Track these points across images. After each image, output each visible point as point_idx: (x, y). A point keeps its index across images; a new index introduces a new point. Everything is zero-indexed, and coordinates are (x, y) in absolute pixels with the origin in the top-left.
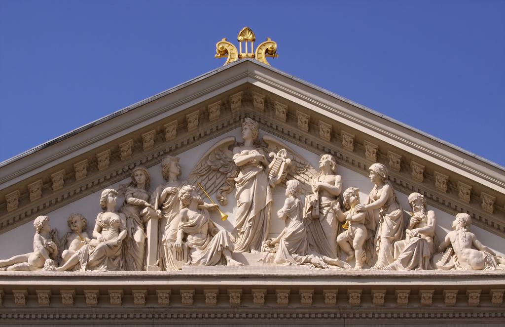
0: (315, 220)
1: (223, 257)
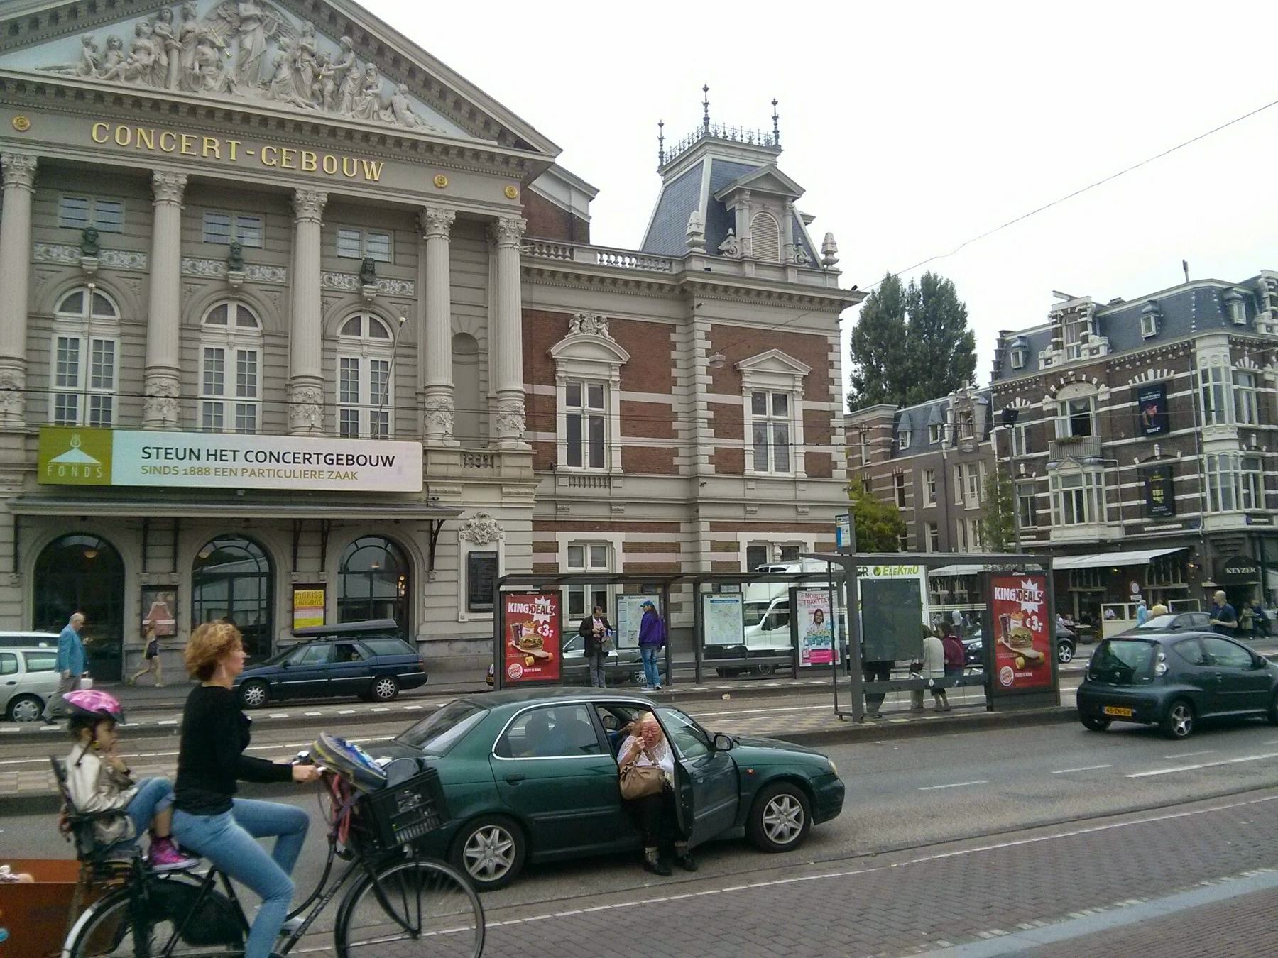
1: (229, 87)
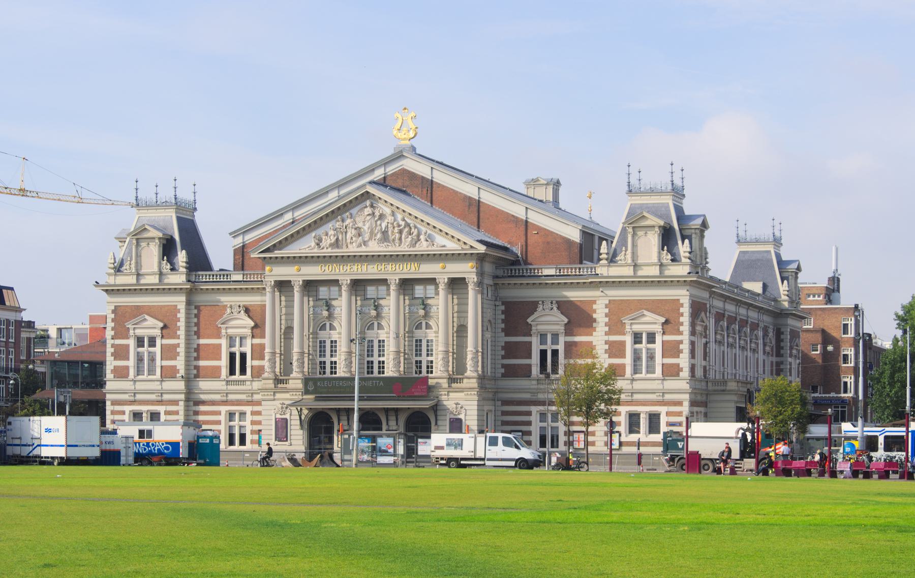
0: (385, 233)
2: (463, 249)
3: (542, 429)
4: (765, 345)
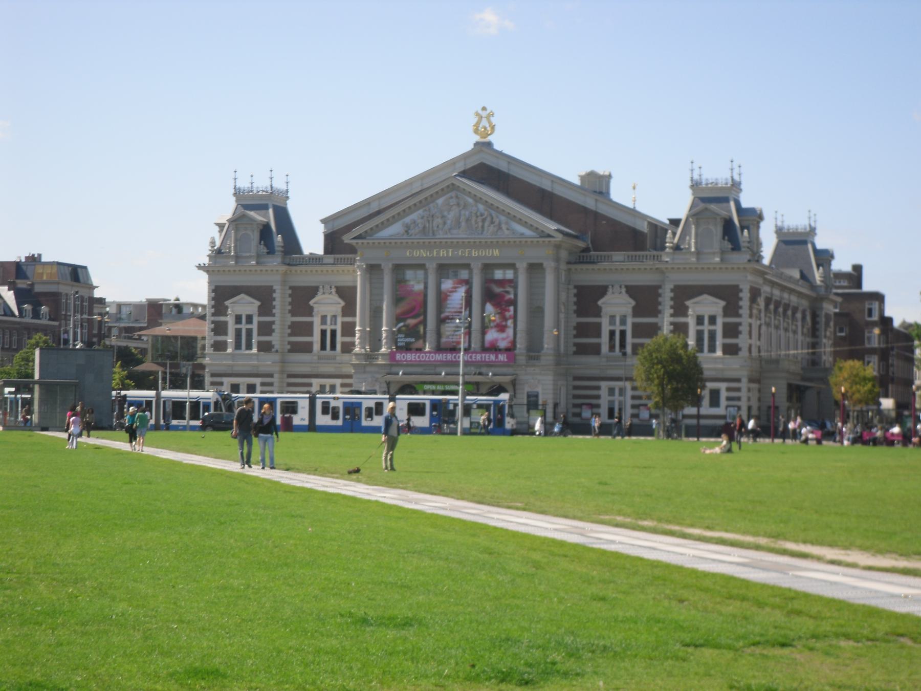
2: (541, 237)
3: (611, 403)
4: (803, 327)
